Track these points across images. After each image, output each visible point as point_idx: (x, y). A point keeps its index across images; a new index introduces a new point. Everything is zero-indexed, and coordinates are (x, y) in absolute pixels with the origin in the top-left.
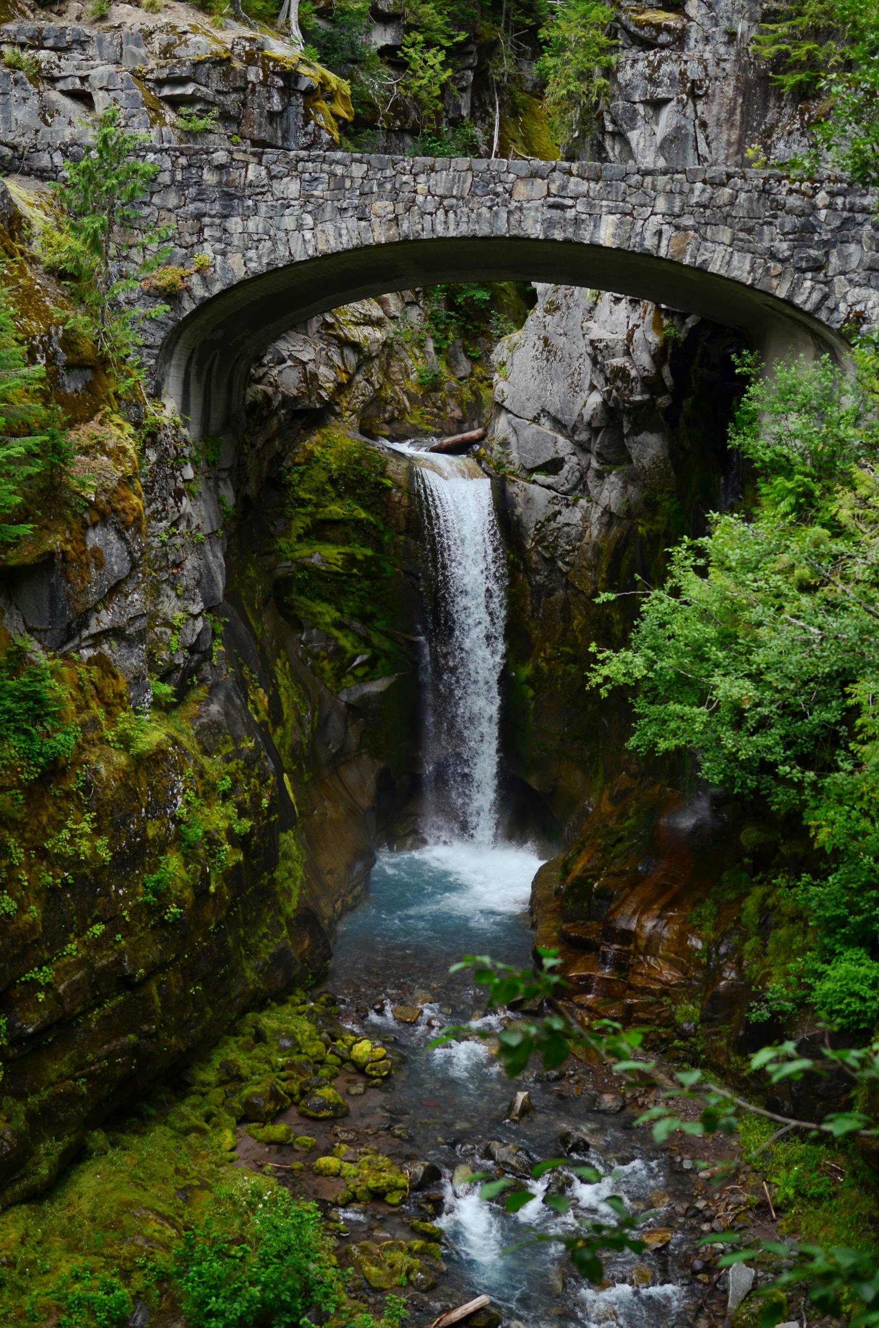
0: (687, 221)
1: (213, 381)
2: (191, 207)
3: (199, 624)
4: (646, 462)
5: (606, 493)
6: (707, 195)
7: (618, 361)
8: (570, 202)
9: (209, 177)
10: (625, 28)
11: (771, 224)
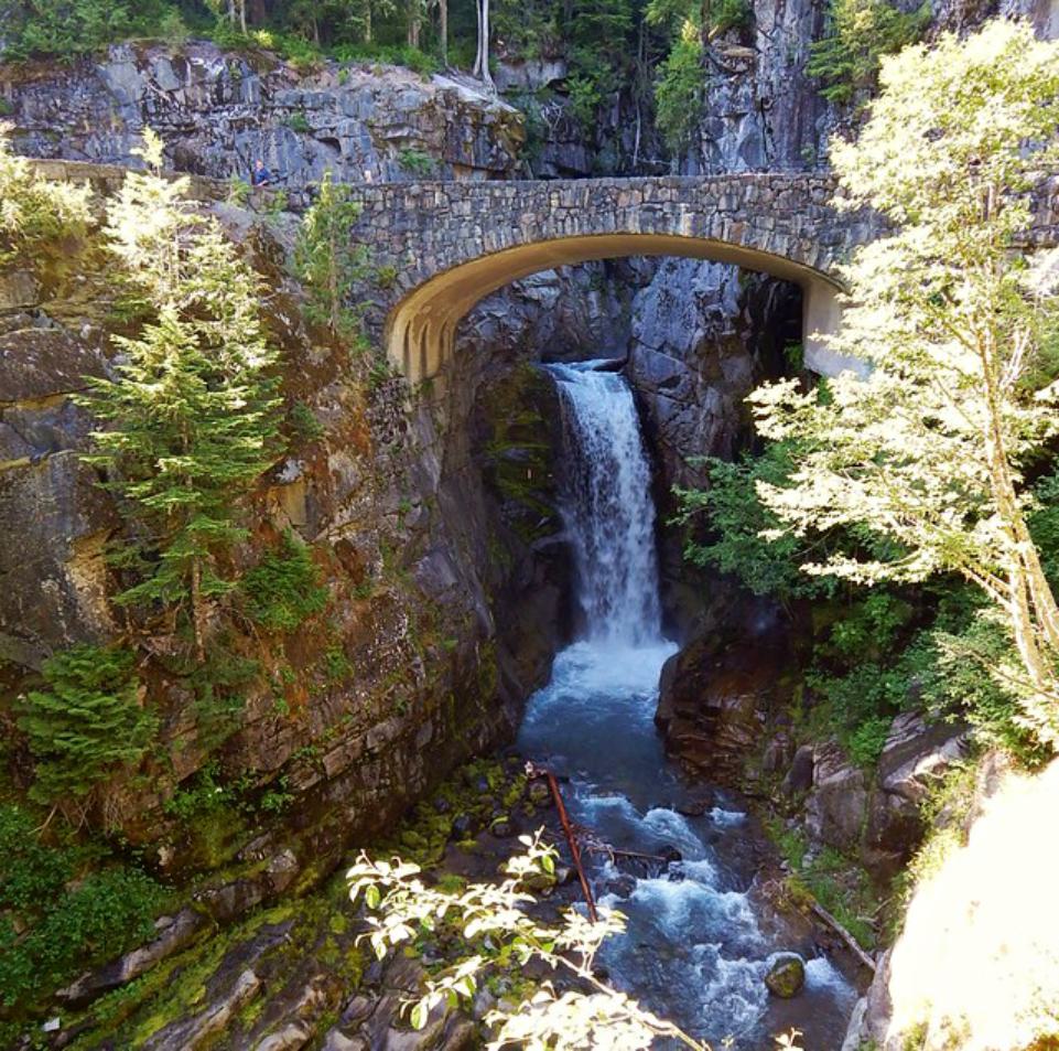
0: (742, 214)
1: (428, 341)
2: (397, 226)
3: (419, 509)
4: (735, 378)
5: (708, 401)
6: (756, 194)
7: (713, 307)
8: (659, 206)
9: (409, 204)
10: (714, 61)
11: (802, 213)
